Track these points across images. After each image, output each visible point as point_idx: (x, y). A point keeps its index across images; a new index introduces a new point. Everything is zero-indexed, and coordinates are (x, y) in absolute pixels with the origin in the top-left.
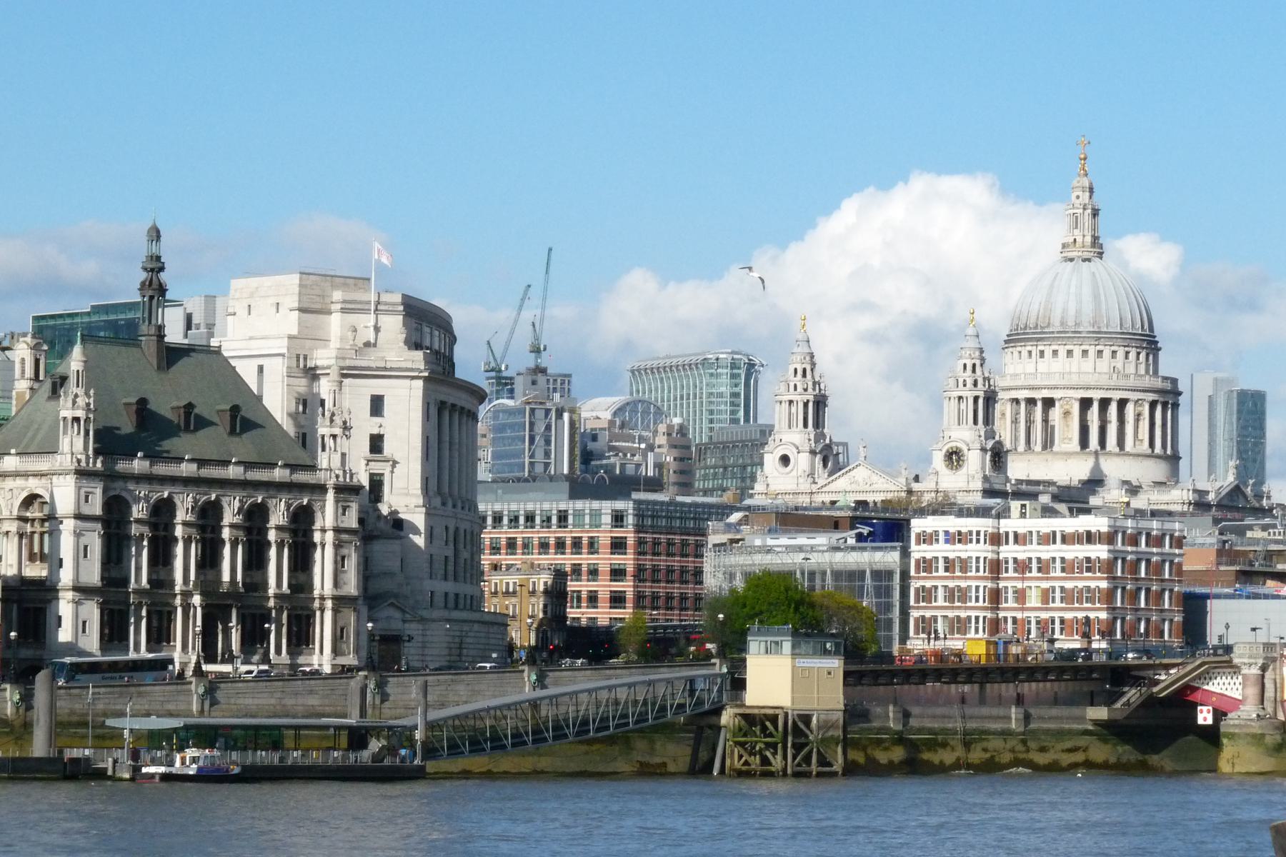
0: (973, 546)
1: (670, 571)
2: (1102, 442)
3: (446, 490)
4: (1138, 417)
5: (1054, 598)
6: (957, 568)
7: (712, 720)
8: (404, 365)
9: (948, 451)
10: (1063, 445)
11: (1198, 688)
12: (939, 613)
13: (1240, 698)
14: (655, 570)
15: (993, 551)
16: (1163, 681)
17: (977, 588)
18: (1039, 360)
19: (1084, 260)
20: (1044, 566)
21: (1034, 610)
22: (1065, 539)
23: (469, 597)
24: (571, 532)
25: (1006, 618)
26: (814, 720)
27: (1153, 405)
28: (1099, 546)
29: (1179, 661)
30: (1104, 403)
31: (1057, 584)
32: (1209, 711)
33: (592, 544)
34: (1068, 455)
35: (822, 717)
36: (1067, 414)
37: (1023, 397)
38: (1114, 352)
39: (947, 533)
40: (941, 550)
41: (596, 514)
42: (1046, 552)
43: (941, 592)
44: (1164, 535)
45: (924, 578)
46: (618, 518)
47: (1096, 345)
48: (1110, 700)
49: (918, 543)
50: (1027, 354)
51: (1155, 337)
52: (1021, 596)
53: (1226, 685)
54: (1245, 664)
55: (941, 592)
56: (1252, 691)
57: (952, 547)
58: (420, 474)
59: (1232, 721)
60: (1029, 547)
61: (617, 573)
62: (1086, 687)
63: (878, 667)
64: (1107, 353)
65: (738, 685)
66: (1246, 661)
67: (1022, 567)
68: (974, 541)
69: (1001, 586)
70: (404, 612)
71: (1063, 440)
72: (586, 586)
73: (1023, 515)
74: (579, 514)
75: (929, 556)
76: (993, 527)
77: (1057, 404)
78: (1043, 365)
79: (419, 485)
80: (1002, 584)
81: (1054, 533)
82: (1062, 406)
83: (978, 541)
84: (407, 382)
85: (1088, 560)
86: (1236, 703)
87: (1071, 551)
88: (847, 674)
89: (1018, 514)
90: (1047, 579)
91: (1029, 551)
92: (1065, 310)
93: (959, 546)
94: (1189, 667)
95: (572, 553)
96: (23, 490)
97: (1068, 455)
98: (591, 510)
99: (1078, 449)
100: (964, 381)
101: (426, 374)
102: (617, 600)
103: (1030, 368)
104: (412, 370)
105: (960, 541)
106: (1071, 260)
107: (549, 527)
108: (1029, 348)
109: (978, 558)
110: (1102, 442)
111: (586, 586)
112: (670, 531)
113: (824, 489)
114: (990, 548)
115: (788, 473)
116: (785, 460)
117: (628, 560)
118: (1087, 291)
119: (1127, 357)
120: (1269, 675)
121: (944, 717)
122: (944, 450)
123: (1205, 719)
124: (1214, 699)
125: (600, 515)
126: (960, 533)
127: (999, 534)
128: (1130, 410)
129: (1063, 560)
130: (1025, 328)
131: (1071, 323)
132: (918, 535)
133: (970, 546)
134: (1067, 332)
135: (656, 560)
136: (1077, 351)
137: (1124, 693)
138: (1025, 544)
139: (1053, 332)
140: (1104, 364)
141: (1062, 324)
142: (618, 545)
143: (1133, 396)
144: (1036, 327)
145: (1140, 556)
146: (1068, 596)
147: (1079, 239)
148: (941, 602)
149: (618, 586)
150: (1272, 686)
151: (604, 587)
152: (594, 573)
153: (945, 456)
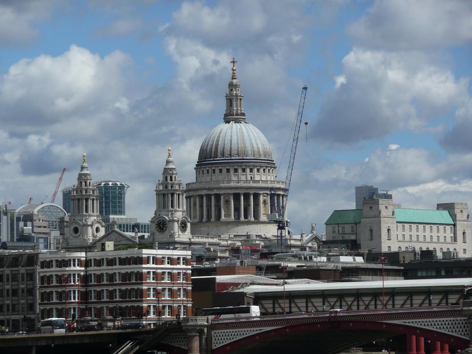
0: (72, 268)
2: (246, 217)
4: (265, 202)
20: (111, 277)
27: (272, 196)
30: (247, 196)
34: (228, 223)
39: (57, 261)
43: (54, 295)
47: (241, 166)
49: (42, 267)
52: (99, 295)
55: (54, 295)
57: (60, 269)
67: (99, 278)
75: (48, 274)
77: (222, 197)
78: (214, 178)
80: (89, 289)
82: (224, 198)
89: (100, 249)
97: (228, 223)
103: (208, 179)
106: (229, 123)
115: (77, 237)
122: (156, 222)
128: (262, 199)
148: (55, 300)
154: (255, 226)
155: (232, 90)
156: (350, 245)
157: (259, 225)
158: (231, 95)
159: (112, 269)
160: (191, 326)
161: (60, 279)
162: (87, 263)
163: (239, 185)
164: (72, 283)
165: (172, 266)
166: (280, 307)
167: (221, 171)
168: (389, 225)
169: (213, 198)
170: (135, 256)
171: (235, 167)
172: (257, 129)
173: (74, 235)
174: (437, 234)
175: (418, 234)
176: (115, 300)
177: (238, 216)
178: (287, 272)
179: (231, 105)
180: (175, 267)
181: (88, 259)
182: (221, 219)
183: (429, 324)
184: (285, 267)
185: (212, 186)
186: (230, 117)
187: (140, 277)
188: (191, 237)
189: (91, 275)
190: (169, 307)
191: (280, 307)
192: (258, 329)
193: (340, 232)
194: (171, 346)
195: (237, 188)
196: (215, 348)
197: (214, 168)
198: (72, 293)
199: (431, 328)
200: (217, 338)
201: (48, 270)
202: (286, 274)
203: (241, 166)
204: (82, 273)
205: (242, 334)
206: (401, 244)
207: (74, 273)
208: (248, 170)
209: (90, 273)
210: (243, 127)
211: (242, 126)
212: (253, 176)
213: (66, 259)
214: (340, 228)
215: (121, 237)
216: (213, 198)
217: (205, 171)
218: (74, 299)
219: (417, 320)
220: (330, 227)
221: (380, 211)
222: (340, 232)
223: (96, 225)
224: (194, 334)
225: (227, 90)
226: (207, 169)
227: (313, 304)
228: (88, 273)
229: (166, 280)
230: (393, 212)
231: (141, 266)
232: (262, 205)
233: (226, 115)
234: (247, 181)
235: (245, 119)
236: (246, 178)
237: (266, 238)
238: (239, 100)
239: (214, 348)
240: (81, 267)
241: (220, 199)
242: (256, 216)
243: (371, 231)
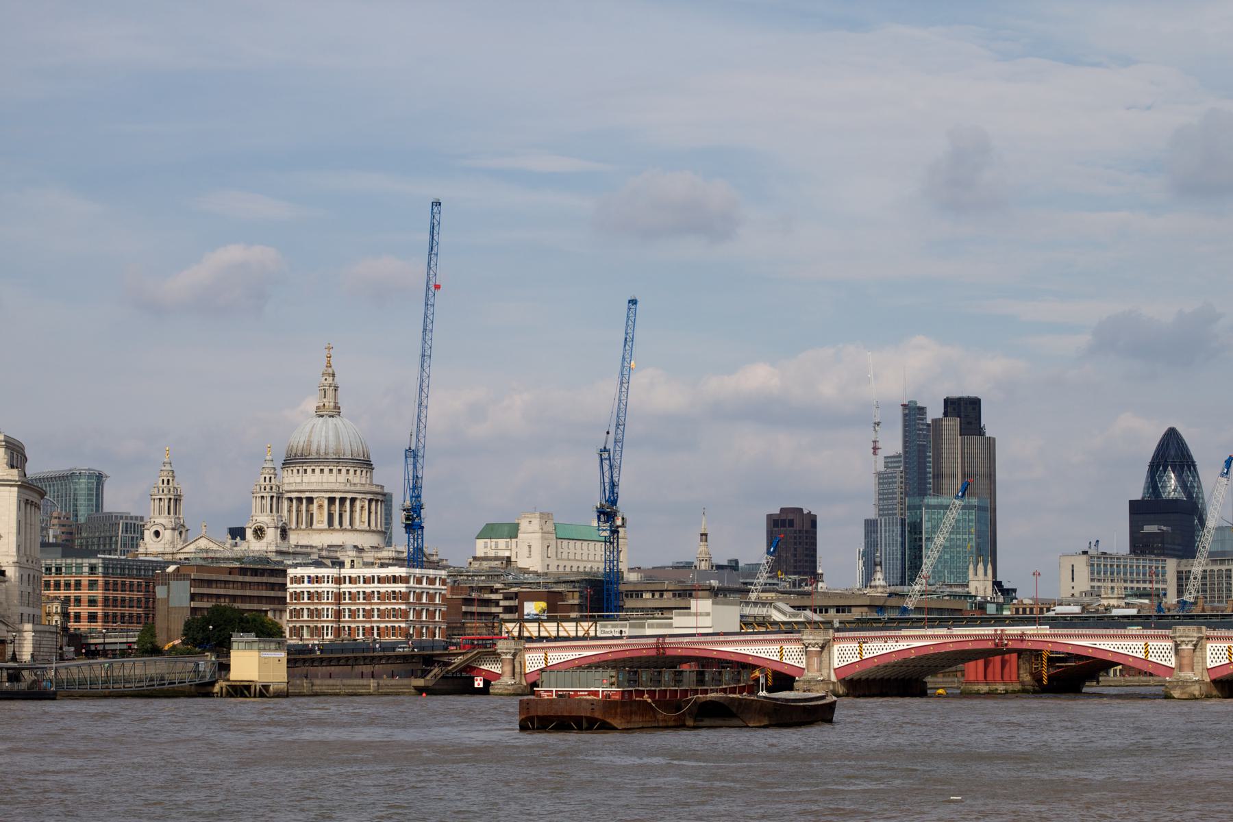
0: (325, 585)
1: (123, 600)
2: (341, 523)
3: (28, 553)
4: (362, 507)
6: (315, 598)
7: (209, 688)
8: (6, 478)
9: (255, 528)
10: (318, 525)
11: (476, 668)
12: (304, 624)
13: (500, 672)
14: (115, 600)
15: (336, 588)
16: (454, 663)
17: (328, 609)
19: (330, 416)
20: (368, 596)
21: (361, 623)
22: (380, 580)
23: (31, 616)
24: (64, 577)
25: (344, 627)
26: (271, 688)
27: (370, 501)
28: (400, 585)
29: (464, 651)
32: (481, 680)
33: (78, 584)
34: (321, 530)
35: (275, 686)
36: (320, 506)
37: (295, 496)
38: (348, 471)
39: (309, 577)
40: (306, 586)
41: (79, 567)
42: (369, 588)
43: (306, 611)
44: (436, 578)
45: (296, 603)
46: (93, 569)
48: (424, 674)
49: (292, 583)
50: (296, 471)
51: (370, 461)
54: (504, 653)
55: (306, 611)
56: (508, 668)
57: (313, 586)
58: (15, 543)
59: (496, 686)
60: (358, 585)
61: (92, 602)
62: (409, 667)
63: (331, 656)
64: (344, 470)
65: (226, 667)
66: (504, 651)
68: (326, 582)
69: (341, 608)
70: (7, 625)
71: (318, 522)
72: (73, 609)
73: (352, 567)
74: (69, 567)
75: (298, 590)
76: (407, 573)
77: (315, 501)
78: (305, 479)
79: (15, 550)
81: (373, 577)
82: (317, 502)
83: (328, 582)
84: (8, 488)
85: (394, 592)
86: (498, 676)
87: (383, 587)
88: (289, 661)
90: (355, 604)
91: (358, 588)
92: (319, 446)
93: (316, 585)
94: (470, 655)
95: (64, 590)
97: (321, 530)
98: (76, 564)
99: (327, 527)
100: (265, 487)
101: (20, 483)
102: (92, 617)
103: (298, 480)
104: (11, 481)
105: (317, 582)
106: (322, 416)
107: (50, 574)
109: (328, 592)
110: (341, 523)
111: (73, 609)
112: (130, 576)
113: (181, 551)
114: (335, 586)
116: (157, 534)
117: (99, 594)
118: (331, 434)
119: (355, 474)
120: (518, 659)
121: (333, 685)
122: (253, 528)
123: (479, 684)
125: (82, 567)
126: (317, 577)
127: (340, 577)
128: (358, 504)
129: (379, 592)
130: (295, 456)
131: (322, 452)
132: (292, 578)
133: (323, 585)
134: (320, 459)
135: (123, 594)
136: (326, 470)
137: (431, 671)
138: (355, 584)
139: (312, 459)
140: (342, 478)
141: (317, 453)
142: (92, 584)
143: (359, 496)
144: (302, 455)
145: (423, 590)
146: (381, 614)
147: (326, 404)
148: (305, 618)
149: (93, 609)
150: (519, 665)
151: (84, 610)
152: (78, 601)
153: (254, 531)
166: (546, 630)
169: (304, 501)
173: (155, 539)
174: (594, 552)
181: (341, 576)
183: (762, 651)
185: (303, 487)
191: (546, 630)
192: (577, 653)
193: (493, 548)
195: (332, 491)
196: (529, 671)
197: (306, 468)
199: (763, 655)
200: (531, 662)
201: (299, 586)
205: (559, 658)
206: (575, 564)
207: (328, 589)
209: (344, 590)
214: (493, 544)
216: (304, 501)
219: (750, 648)
222: (493, 548)
226: (298, 468)
227: (545, 628)
228: (341, 590)
239: (527, 671)
241: (312, 503)
243: (530, 547)
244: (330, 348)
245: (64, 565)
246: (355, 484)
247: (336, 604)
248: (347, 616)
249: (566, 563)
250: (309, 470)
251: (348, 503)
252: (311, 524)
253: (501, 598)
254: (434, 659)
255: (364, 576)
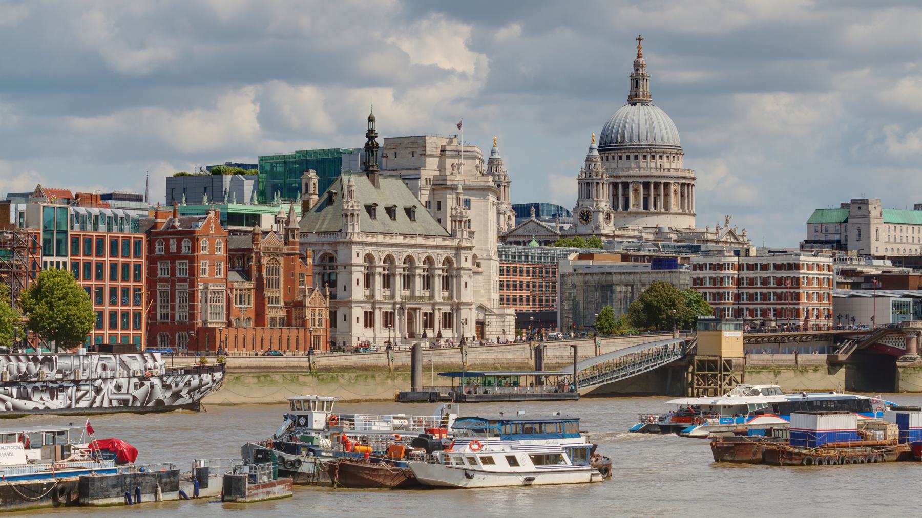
0: (727, 271)
4: (675, 191)
5: (824, 299)
13: (904, 349)
17: (729, 293)
18: (619, 161)
20: (765, 282)
30: (657, 185)
31: (758, 291)
34: (637, 214)
39: (711, 264)
42: (764, 274)
45: (699, 288)
47: (650, 153)
50: (611, 158)
53: (893, 343)
67: (752, 282)
75: (701, 276)
77: (630, 186)
80: (741, 291)
82: (633, 187)
88: (745, 338)
96: (320, 251)
106: (635, 105)
108: (613, 154)
113: (512, 235)
122: (579, 213)
124: (889, 350)
128: (672, 188)
139: (626, 146)
143: (672, 181)
154: (665, 217)
155: (637, 70)
156: (835, 245)
157: (669, 216)
158: (638, 75)
159: (766, 274)
160: (912, 328)
161: (714, 281)
162: (740, 267)
163: (649, 173)
164: (727, 286)
165: (819, 272)
167: (628, 157)
168: (877, 226)
169: (620, 186)
170: (792, 262)
171: (644, 154)
172: (663, 112)
175: (908, 235)
176: (755, 302)
177: (646, 207)
178: (862, 277)
179: (637, 86)
180: (821, 273)
182: (629, 210)
184: (862, 272)
186: (633, 99)
187: (796, 281)
188: (614, 229)
189: (743, 278)
190: (827, 309)
193: (823, 231)
194: (885, 345)
195: (647, 177)
198: (727, 294)
202: (863, 278)
203: (650, 153)
204: (736, 276)
208: (657, 157)
209: (743, 276)
210: (651, 111)
211: (650, 109)
212: (662, 164)
213: (721, 263)
215: (539, 228)
216: (620, 186)
217: (609, 158)
218: (728, 300)
220: (813, 226)
221: (869, 212)
222: (823, 231)
223: (508, 214)
224: (913, 335)
225: (632, 70)
228: (740, 277)
229: (815, 285)
230: (881, 213)
231: (797, 271)
232: (672, 195)
233: (630, 97)
234: (656, 168)
235: (651, 101)
236: (656, 166)
237: (676, 231)
238: (645, 80)
240: (734, 270)
241: (628, 188)
242: (667, 206)
243: (859, 231)
244: (639, 39)
245: (523, 254)
246: (669, 170)
247: (736, 288)
248: (745, 298)
249: (893, 246)
250: (624, 157)
251: (662, 186)
252: (626, 207)
253: (863, 281)
254: (844, 337)
255: (760, 264)
